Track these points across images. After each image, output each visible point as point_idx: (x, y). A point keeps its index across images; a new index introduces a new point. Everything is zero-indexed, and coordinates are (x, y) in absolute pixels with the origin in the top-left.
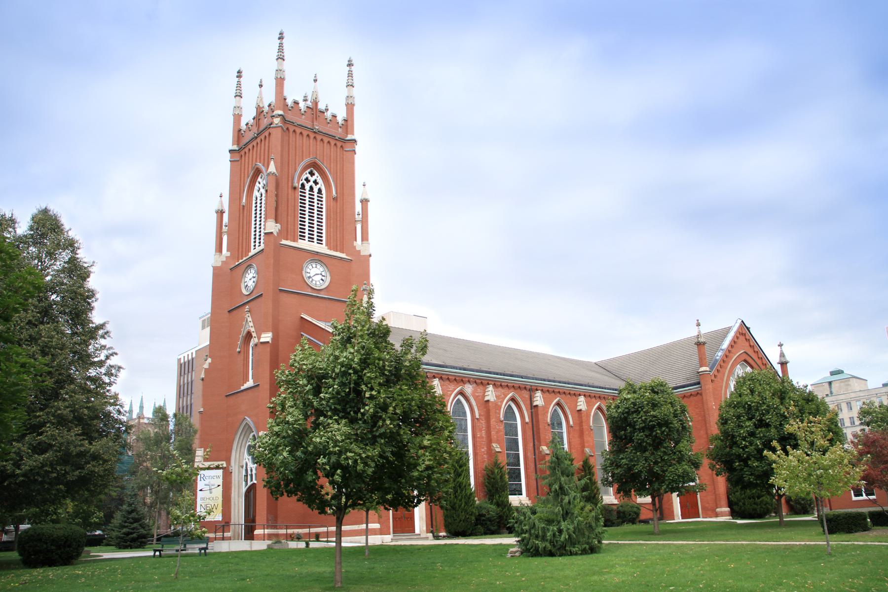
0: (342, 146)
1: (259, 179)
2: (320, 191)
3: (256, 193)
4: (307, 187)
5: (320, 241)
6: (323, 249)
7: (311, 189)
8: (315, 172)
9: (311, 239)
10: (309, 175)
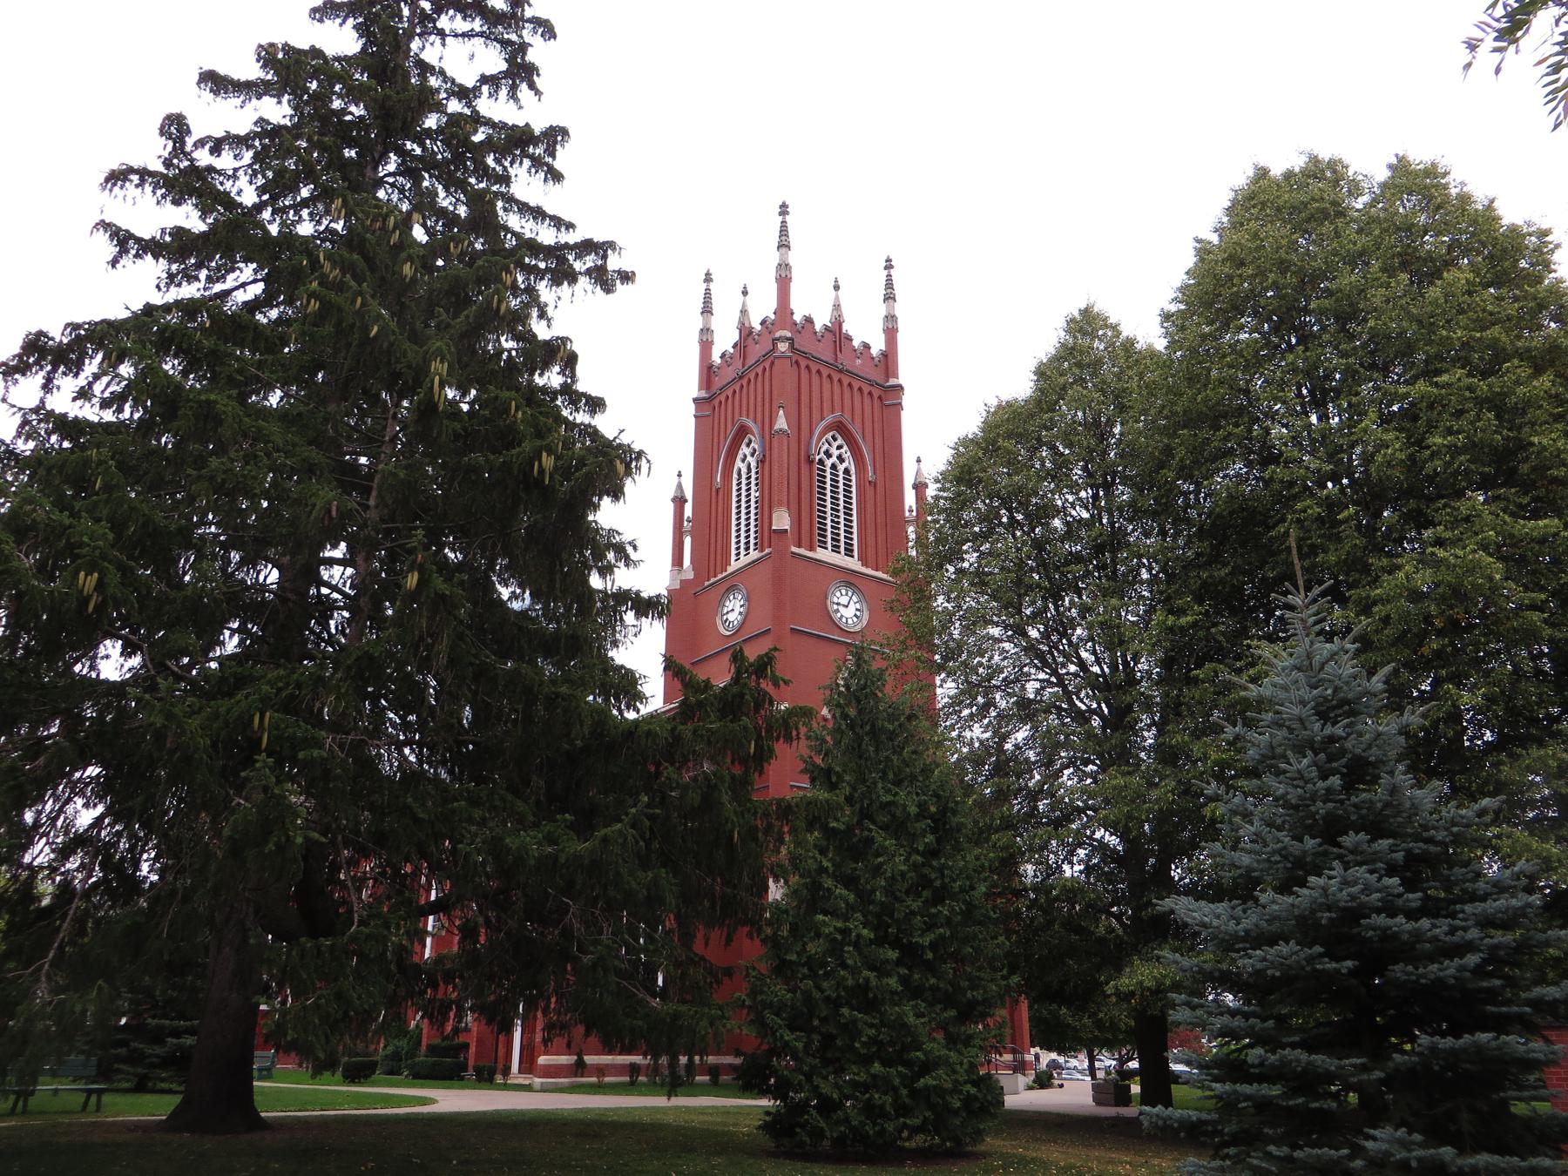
0: (880, 397)
4: (829, 463)
5: (849, 552)
6: (854, 563)
7: (834, 467)
8: (838, 436)
9: (836, 549)
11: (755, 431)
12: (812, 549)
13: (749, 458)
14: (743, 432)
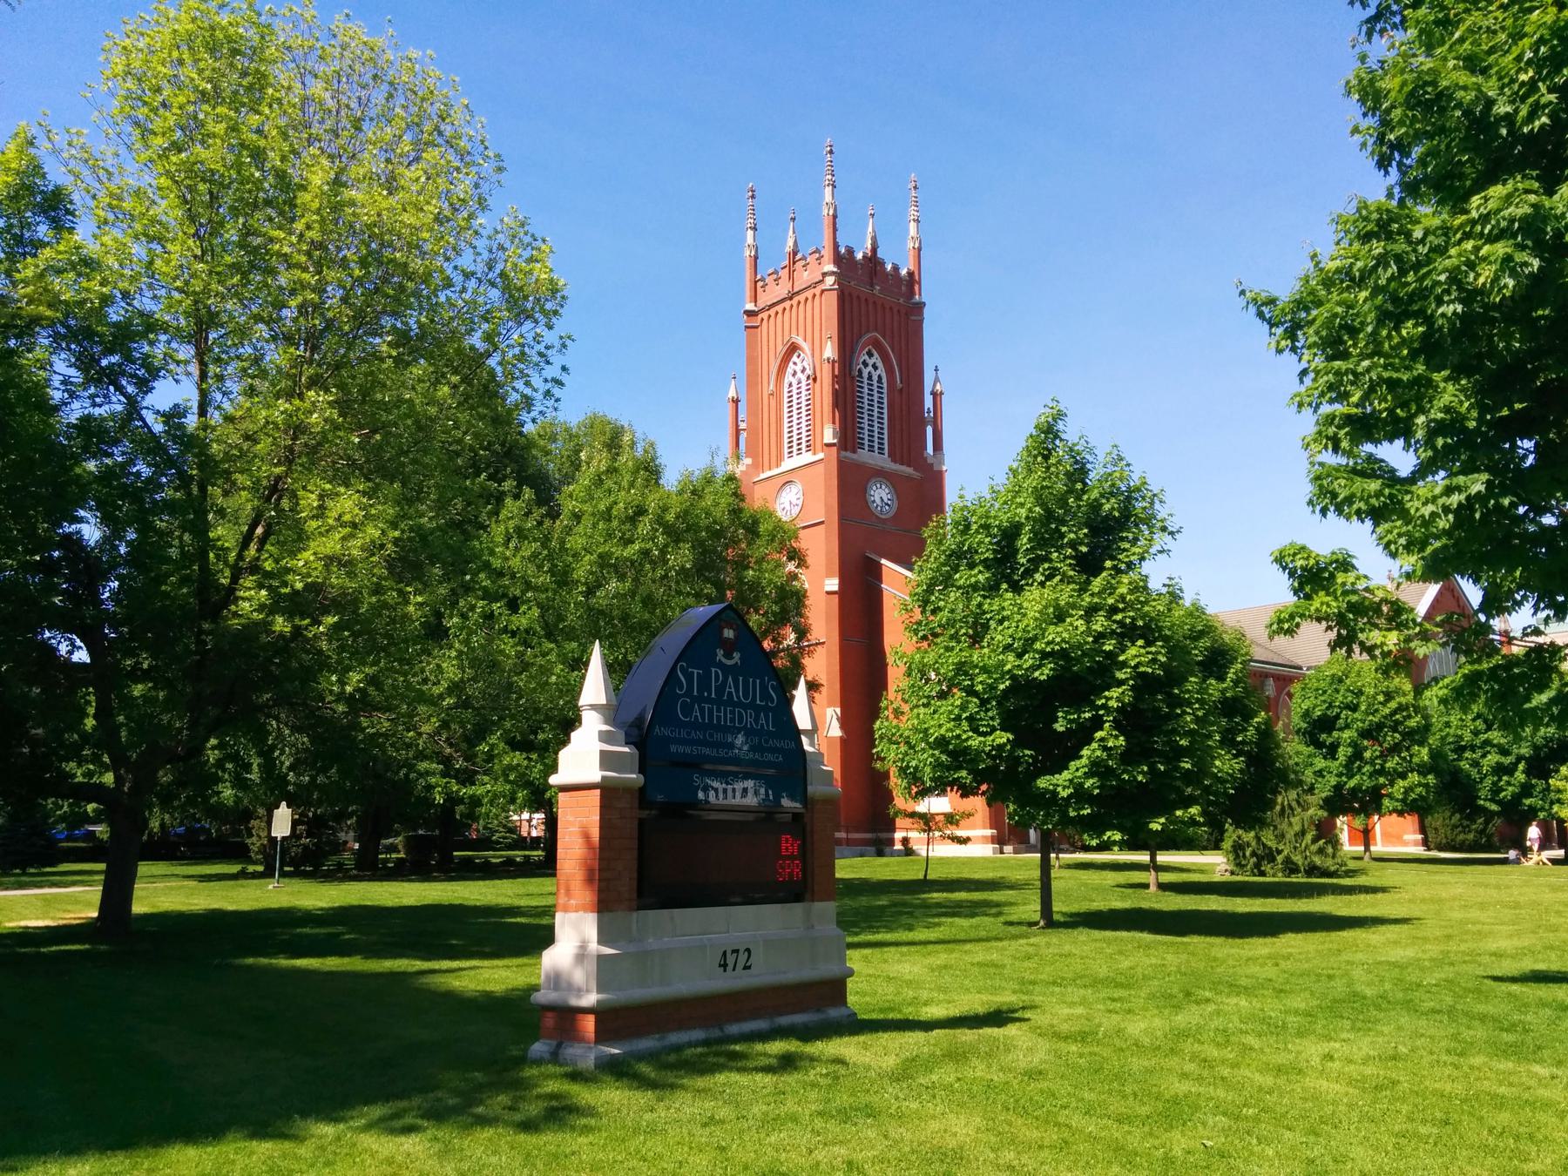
1: (795, 358)
2: (880, 377)
3: (788, 378)
4: (865, 375)
6: (883, 461)
10: (866, 357)
11: (805, 346)
12: (854, 452)
13: (799, 375)
14: (793, 349)
